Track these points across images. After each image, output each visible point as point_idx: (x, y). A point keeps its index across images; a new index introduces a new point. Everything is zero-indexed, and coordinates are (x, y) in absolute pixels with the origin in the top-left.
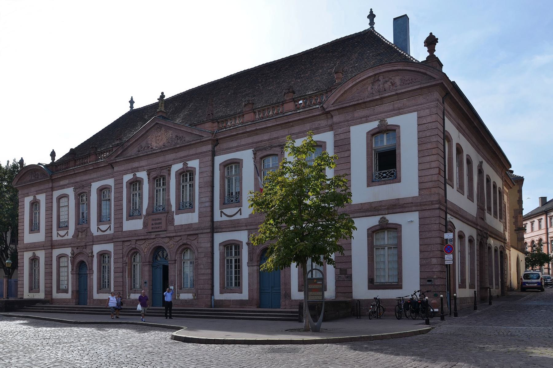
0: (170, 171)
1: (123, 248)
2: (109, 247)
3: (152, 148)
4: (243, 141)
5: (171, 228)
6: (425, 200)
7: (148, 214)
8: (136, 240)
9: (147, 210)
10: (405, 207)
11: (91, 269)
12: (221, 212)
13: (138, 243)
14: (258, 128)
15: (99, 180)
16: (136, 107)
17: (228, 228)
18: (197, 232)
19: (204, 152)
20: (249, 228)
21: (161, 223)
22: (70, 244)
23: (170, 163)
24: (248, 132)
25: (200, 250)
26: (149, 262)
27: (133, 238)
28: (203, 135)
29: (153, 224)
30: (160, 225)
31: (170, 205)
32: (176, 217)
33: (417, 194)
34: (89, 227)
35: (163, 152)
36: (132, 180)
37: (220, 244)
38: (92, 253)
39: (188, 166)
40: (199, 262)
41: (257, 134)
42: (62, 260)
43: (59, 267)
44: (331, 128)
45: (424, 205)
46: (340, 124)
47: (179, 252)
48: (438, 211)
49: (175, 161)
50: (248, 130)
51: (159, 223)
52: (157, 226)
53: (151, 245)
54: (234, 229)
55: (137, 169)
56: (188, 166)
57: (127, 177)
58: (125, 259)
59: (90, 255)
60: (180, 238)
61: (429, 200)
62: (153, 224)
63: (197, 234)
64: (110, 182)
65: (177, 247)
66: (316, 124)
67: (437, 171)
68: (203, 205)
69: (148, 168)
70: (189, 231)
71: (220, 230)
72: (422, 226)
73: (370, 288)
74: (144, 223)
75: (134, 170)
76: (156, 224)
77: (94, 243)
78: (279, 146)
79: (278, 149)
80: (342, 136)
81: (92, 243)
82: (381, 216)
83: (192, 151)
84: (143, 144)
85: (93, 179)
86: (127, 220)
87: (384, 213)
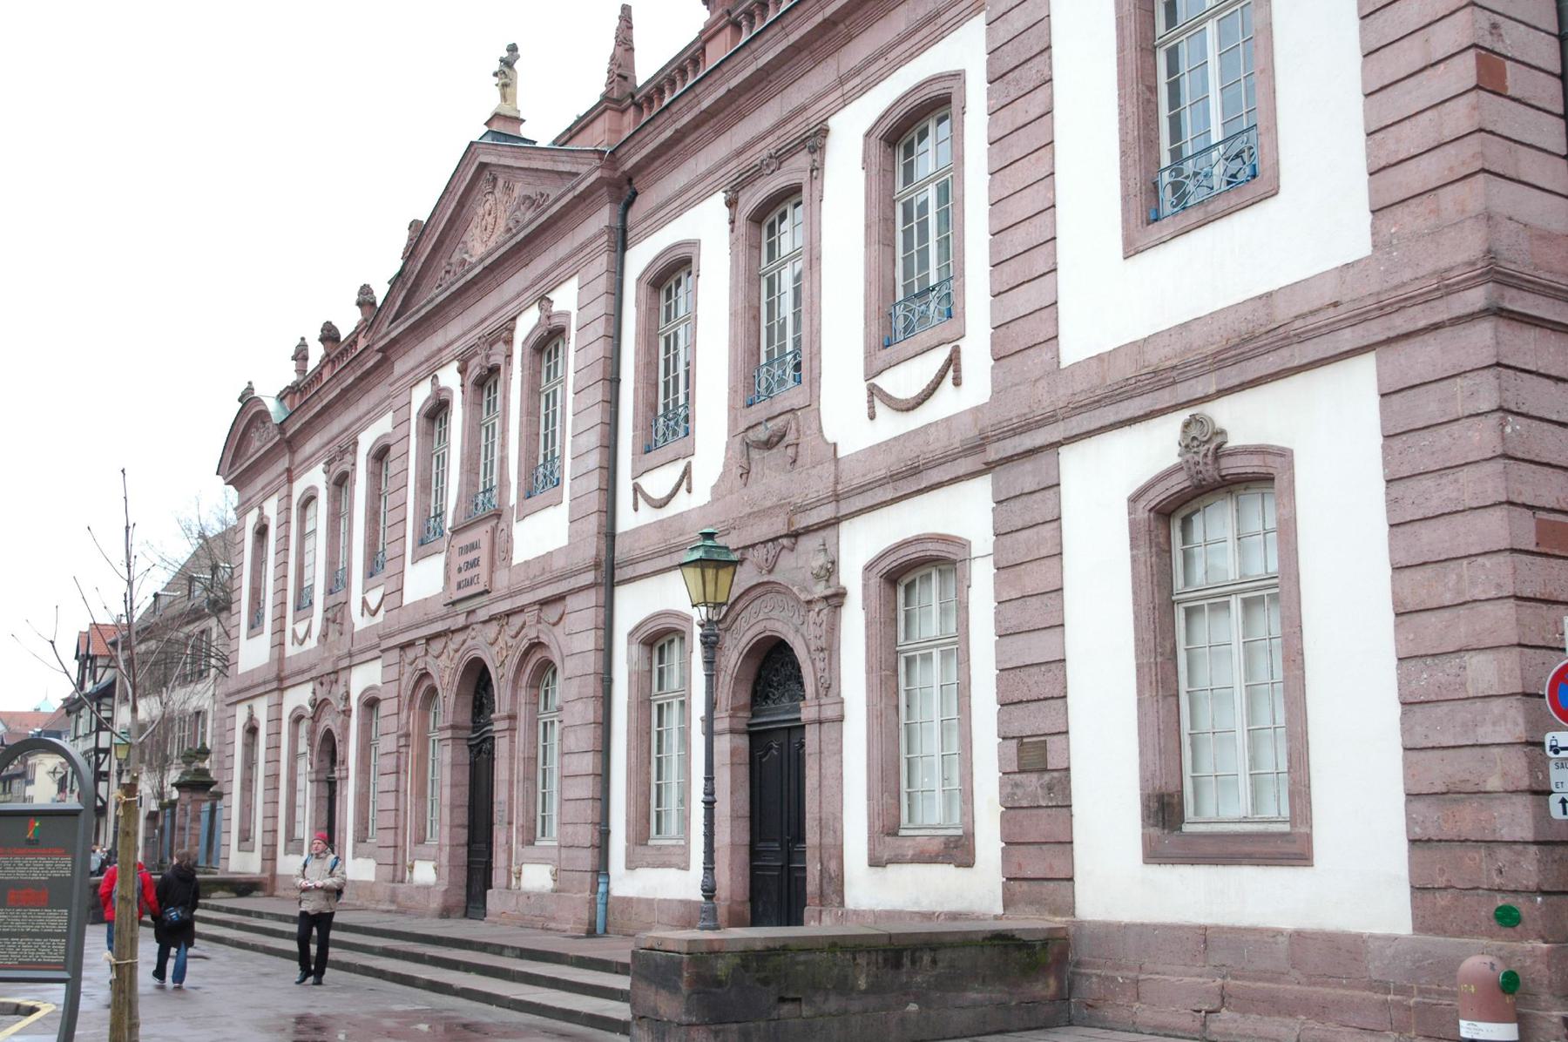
1: (401, 674)
5: (502, 581)
6: (1407, 275)
7: (456, 532)
10: (1302, 338)
13: (436, 646)
14: (734, 83)
26: (453, 727)
31: (504, 482)
33: (1361, 247)
39: (555, 309)
42: (304, 727)
43: (294, 756)
45: (1402, 305)
47: (525, 678)
48: (1484, 332)
50: (705, 104)
57: (421, 395)
58: (404, 715)
61: (1429, 267)
63: (560, 598)
64: (383, 426)
65: (516, 661)
67: (1465, 71)
69: (458, 347)
72: (1397, 443)
73: (1154, 855)
79: (803, 159)
80: (1018, 20)
82: (1185, 415)
87: (1200, 387)
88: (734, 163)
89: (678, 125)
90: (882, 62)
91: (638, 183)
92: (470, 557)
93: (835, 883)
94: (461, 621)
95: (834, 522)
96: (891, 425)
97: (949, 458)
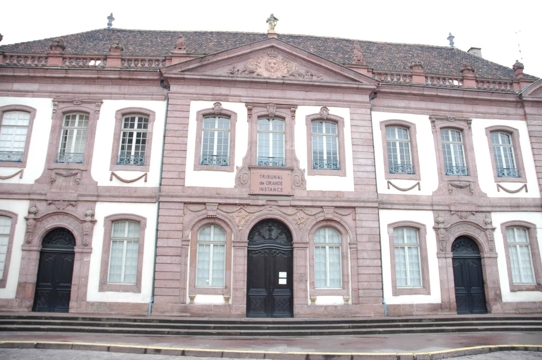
0: (294, 112)
2: (148, 211)
3: (258, 75)
4: (423, 105)
5: (298, 193)
8: (220, 204)
9: (245, 158)
11: (87, 245)
12: (389, 182)
13: (224, 208)
14: (439, 94)
15: (125, 98)
16: (116, 25)
17: (404, 204)
18: (354, 205)
19: (361, 102)
20: (435, 208)
21: (281, 183)
22: (29, 194)
23: (295, 102)
24: (423, 95)
25: (359, 231)
27: (212, 200)
28: (361, 80)
29: (263, 183)
30: (280, 186)
32: (307, 177)
34: (87, 171)
35: (284, 85)
36: (212, 111)
37: (389, 225)
38: (93, 215)
40: (359, 248)
41: (432, 101)
44: (525, 117)
46: (535, 116)
49: (306, 102)
50: (425, 93)
51: (277, 183)
52: (273, 187)
53: (253, 216)
54: (411, 207)
55: (226, 98)
56: (330, 112)
59: (89, 218)
60: (319, 210)
62: (263, 183)
63: (354, 208)
66: (504, 110)
68: (362, 169)
70: (340, 201)
71: (389, 206)
74: (238, 179)
75: (218, 99)
76: (270, 183)
77: (101, 199)
78: (465, 120)
81: (94, 199)
83: (335, 96)
84: (240, 66)
85: (111, 94)
86: (196, 168)
88: (431, 111)
89: (411, 92)
90: (491, 115)
91: (378, 95)
92: (278, 180)
93: (499, 296)
94: (263, 202)
95: (490, 212)
96: (503, 194)
97: (528, 206)
